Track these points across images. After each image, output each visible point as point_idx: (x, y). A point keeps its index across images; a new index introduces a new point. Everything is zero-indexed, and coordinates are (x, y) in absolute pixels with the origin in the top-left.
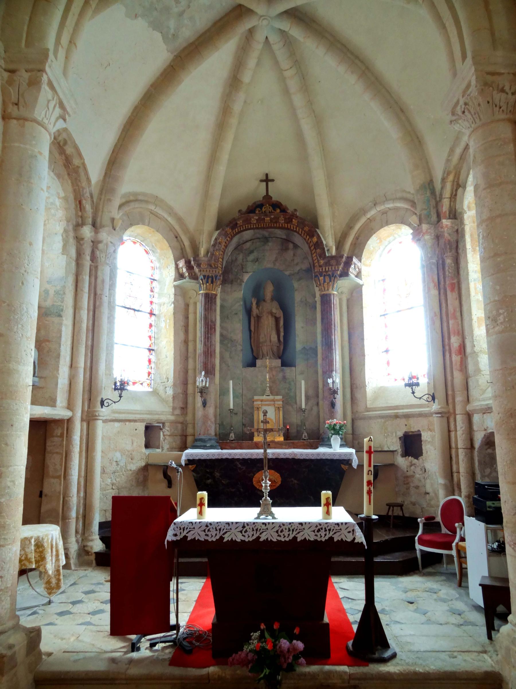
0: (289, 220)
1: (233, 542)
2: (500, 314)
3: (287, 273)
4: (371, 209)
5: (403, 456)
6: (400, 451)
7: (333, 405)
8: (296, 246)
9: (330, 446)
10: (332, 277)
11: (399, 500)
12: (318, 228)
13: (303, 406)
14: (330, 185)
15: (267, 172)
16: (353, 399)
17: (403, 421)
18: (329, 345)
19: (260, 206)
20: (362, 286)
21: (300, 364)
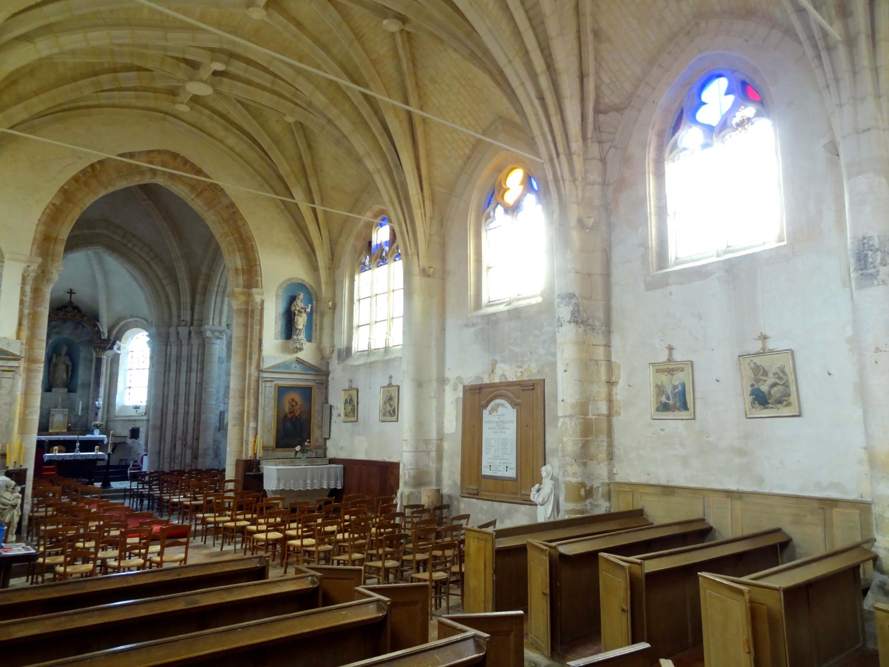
0: (83, 317)
1: (67, 460)
3: (77, 341)
4: (130, 318)
5: (130, 438)
6: (129, 436)
7: (97, 414)
8: (84, 327)
9: (93, 434)
10: (104, 349)
11: (126, 458)
12: (98, 321)
13: (80, 414)
14: (108, 301)
15: (71, 287)
16: (108, 411)
17: (132, 423)
18: (98, 384)
19: (66, 307)
20: (119, 354)
21: (80, 391)
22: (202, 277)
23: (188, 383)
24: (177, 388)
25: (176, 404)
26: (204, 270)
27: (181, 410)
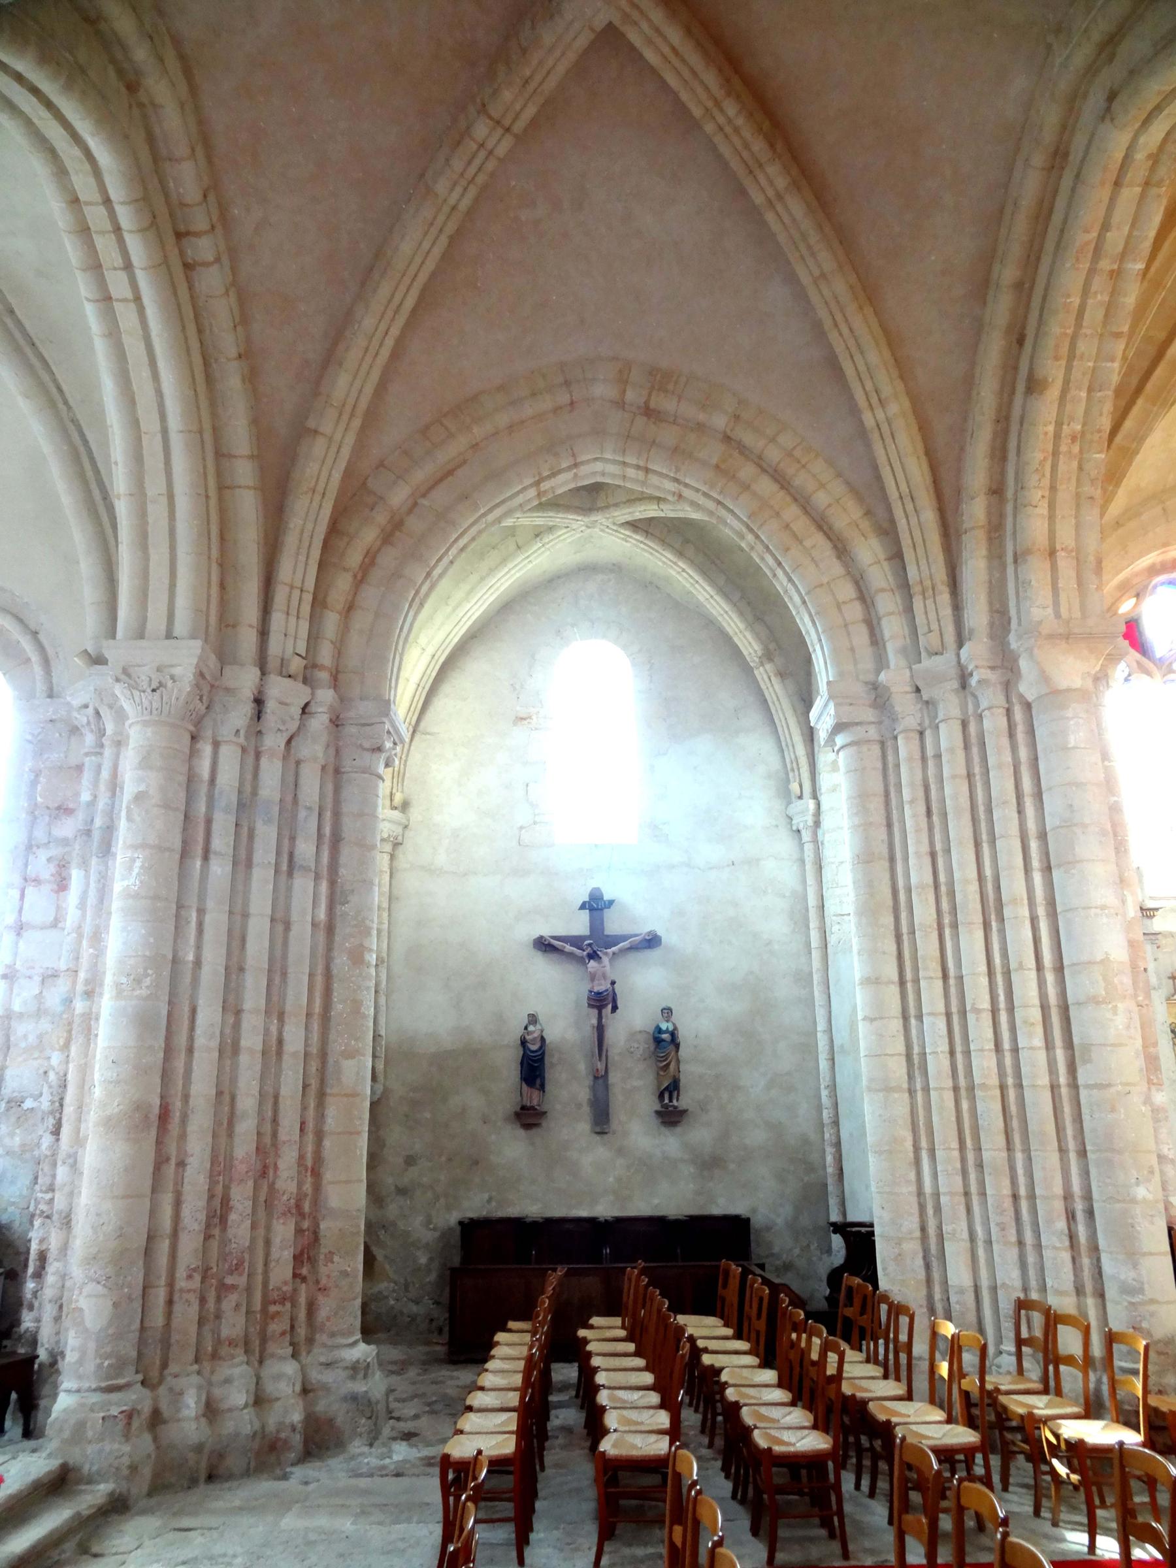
2: (148, 975)
22: (381, 518)
23: (281, 922)
24: (237, 940)
25: (232, 1009)
26: (399, 497)
27: (251, 1040)
